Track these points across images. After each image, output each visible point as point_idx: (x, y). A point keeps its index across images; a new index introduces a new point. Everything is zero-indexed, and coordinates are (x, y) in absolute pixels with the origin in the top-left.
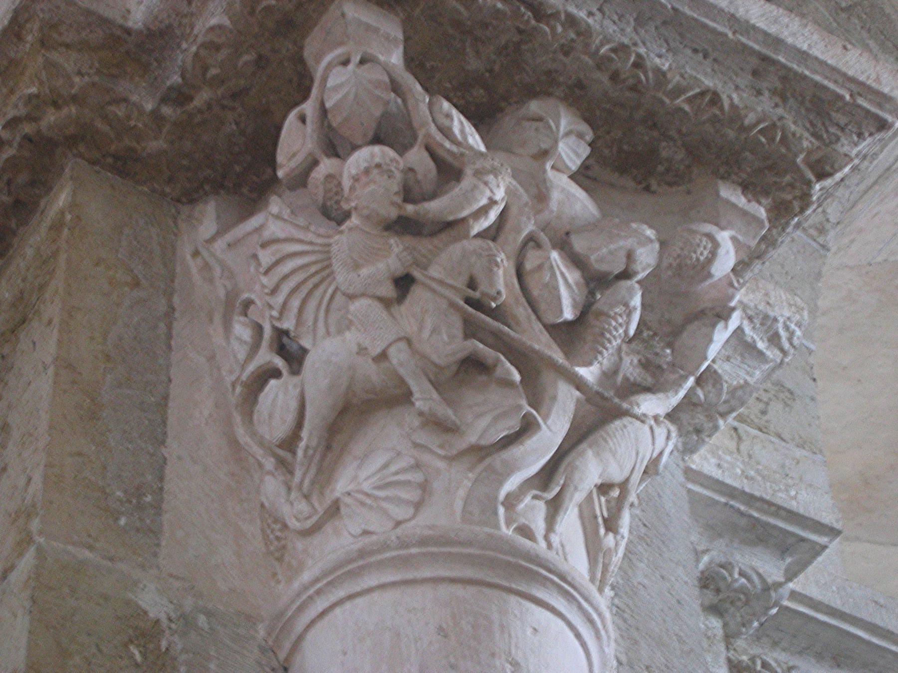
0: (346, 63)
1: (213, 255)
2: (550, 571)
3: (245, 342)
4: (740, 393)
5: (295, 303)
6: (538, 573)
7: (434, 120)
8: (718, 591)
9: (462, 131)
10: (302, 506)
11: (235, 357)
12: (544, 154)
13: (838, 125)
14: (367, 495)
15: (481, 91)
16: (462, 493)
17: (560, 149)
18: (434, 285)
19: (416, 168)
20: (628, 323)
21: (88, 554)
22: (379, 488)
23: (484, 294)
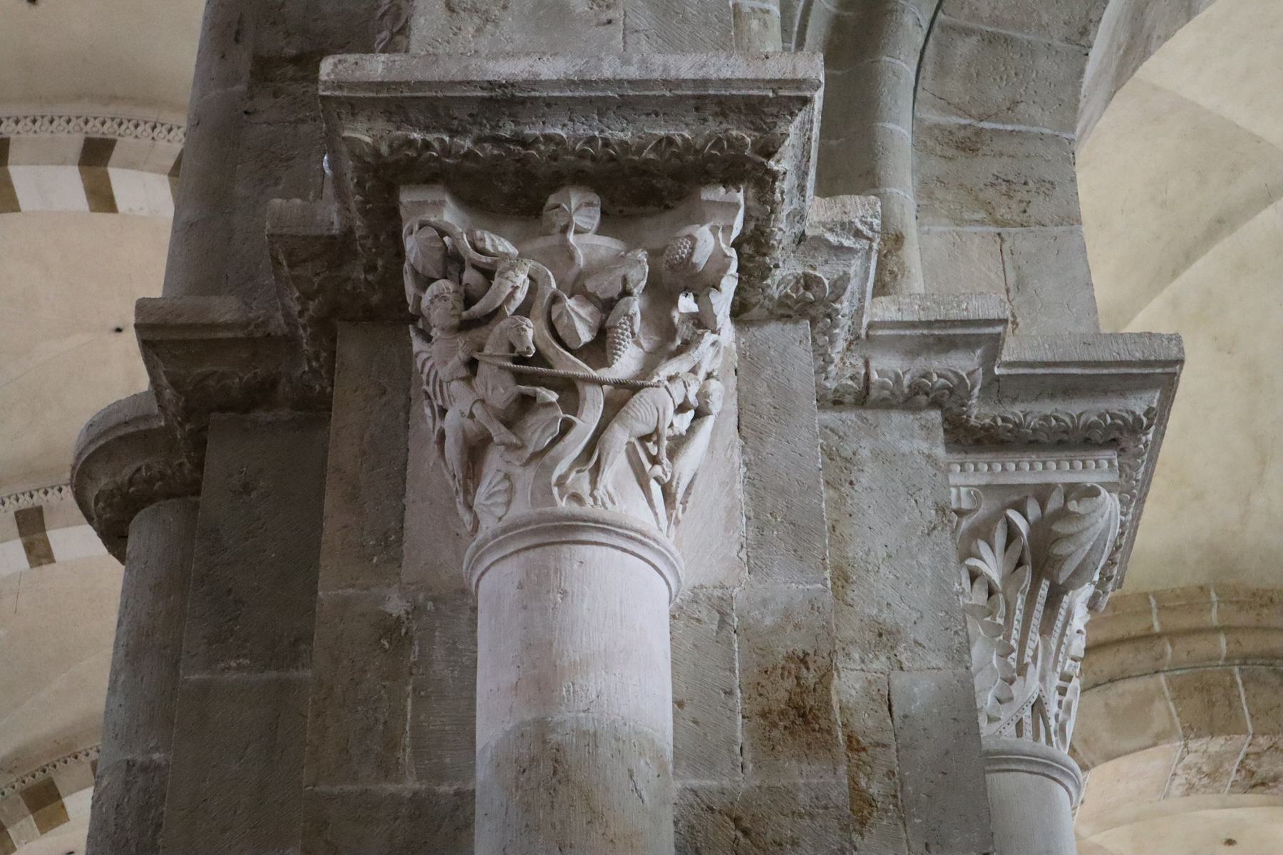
0: (411, 233)
2: (585, 521)
4: (839, 283)
6: (577, 526)
8: (927, 394)
9: (494, 246)
12: (565, 230)
13: (772, 115)
20: (631, 327)
21: (351, 591)
22: (487, 499)
23: (518, 353)
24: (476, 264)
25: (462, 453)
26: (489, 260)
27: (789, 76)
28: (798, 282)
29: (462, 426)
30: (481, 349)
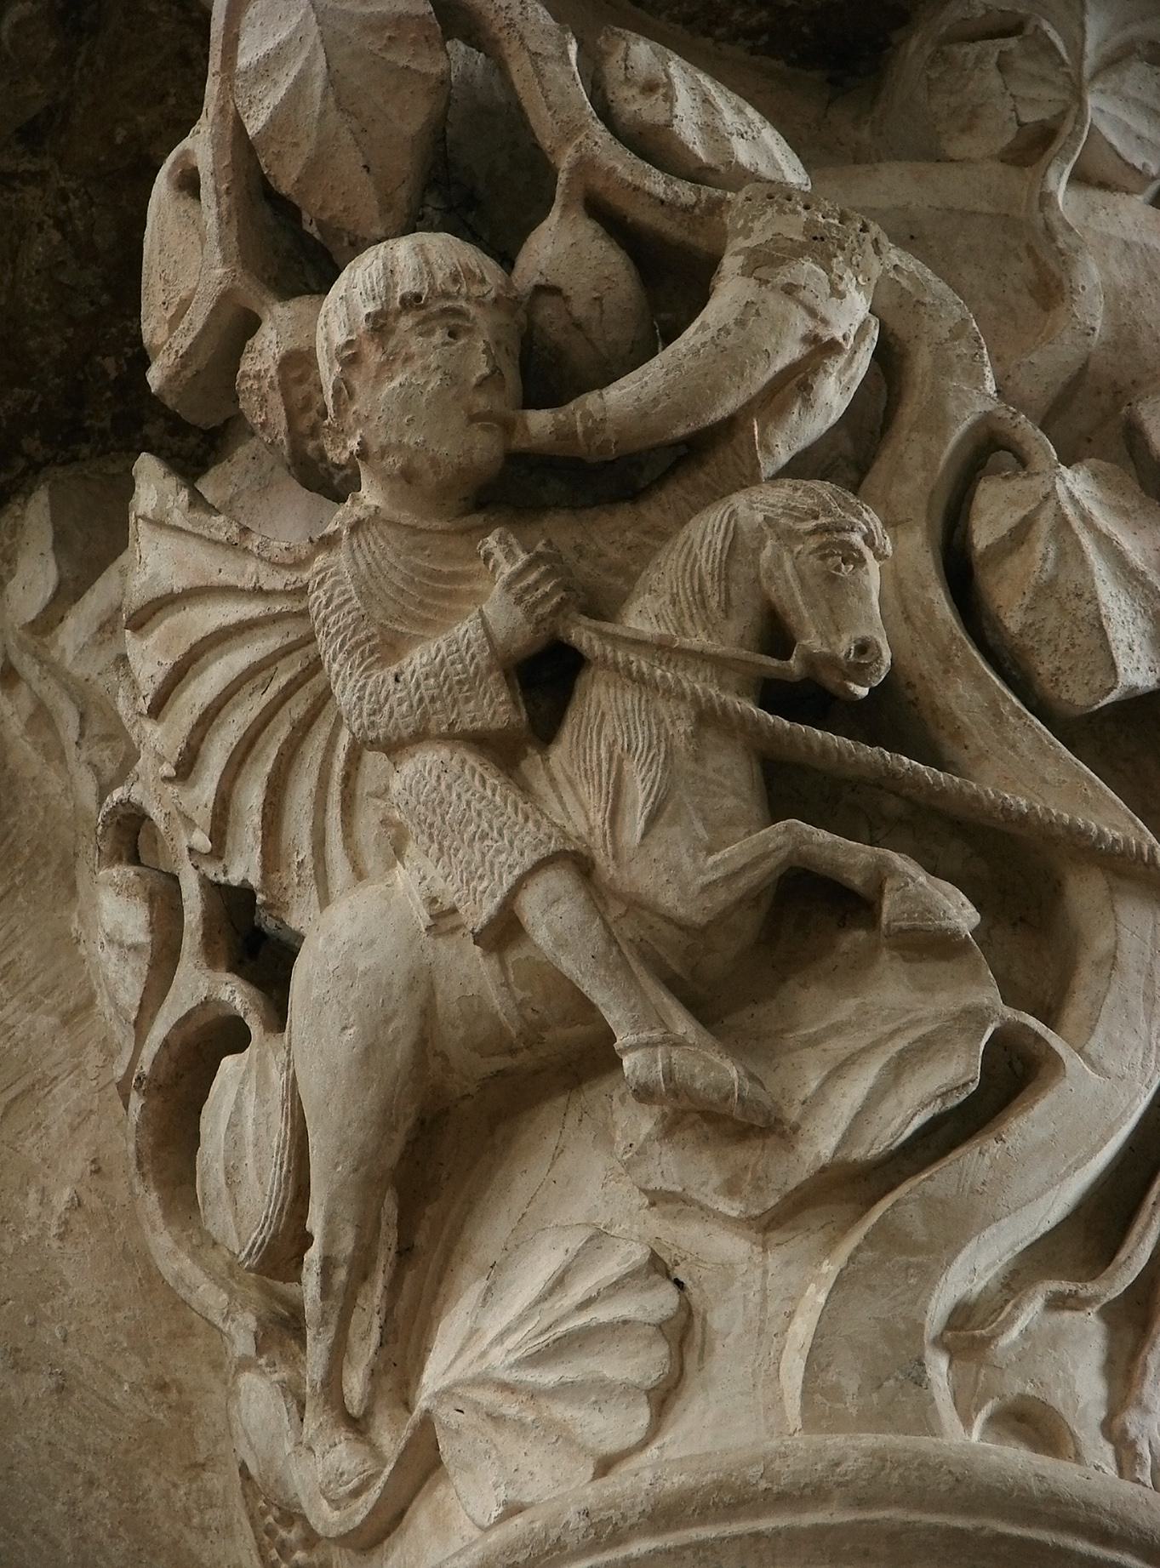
1: (53, 669)
3: (135, 948)
5: (252, 796)
7: (606, 113)
9: (711, 130)
14: (505, 1387)
16: (802, 1329)
22: (537, 1359)
23: (810, 660)
24: (620, 201)
25: (386, 1120)
26: (685, 192)
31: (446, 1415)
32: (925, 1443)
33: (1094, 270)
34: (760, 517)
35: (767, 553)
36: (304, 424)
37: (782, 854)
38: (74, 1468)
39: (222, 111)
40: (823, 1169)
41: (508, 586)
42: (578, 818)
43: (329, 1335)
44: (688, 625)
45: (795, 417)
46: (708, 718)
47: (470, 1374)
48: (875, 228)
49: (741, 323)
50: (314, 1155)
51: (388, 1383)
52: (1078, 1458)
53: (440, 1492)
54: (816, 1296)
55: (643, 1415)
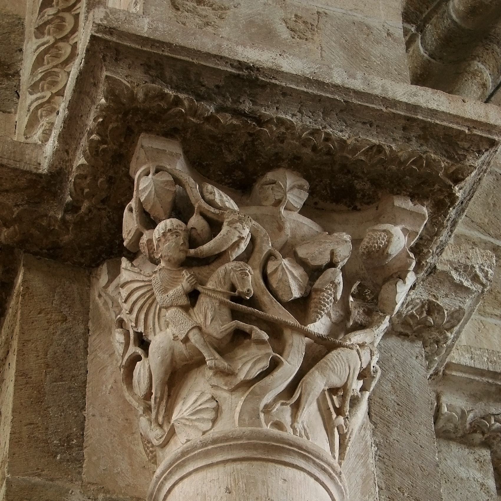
0: (147, 174)
1: (107, 295)
2: (291, 445)
3: (122, 343)
4: (456, 315)
5: (142, 317)
6: (283, 448)
7: (203, 197)
8: (483, 433)
9: (221, 201)
10: (158, 432)
11: (118, 353)
12: (278, 203)
13: (464, 149)
15: (240, 172)
16: (238, 409)
17: (288, 198)
18: (210, 293)
19: (196, 227)
20: (335, 293)
21: (37, 479)
22: (192, 414)
23: (239, 292)
24: (205, 213)
25: (166, 372)
26: (217, 211)
27: (483, 120)
28: (423, 306)
29: (172, 349)
30: (203, 283)
31: (176, 424)
32: (260, 429)
33: (288, 225)
34: (230, 268)
35: (231, 274)
36: (151, 252)
37: (235, 326)
38: (111, 434)
39: (137, 197)
40: (242, 381)
41: (187, 280)
42: (199, 320)
43: (156, 411)
44: (218, 286)
45: (236, 250)
46: (221, 303)
47: (181, 417)
48: (250, 218)
49: (227, 234)
50: (153, 379)
51: (166, 418)
52: (286, 431)
53: (176, 437)
54: (241, 403)
55: (211, 424)
